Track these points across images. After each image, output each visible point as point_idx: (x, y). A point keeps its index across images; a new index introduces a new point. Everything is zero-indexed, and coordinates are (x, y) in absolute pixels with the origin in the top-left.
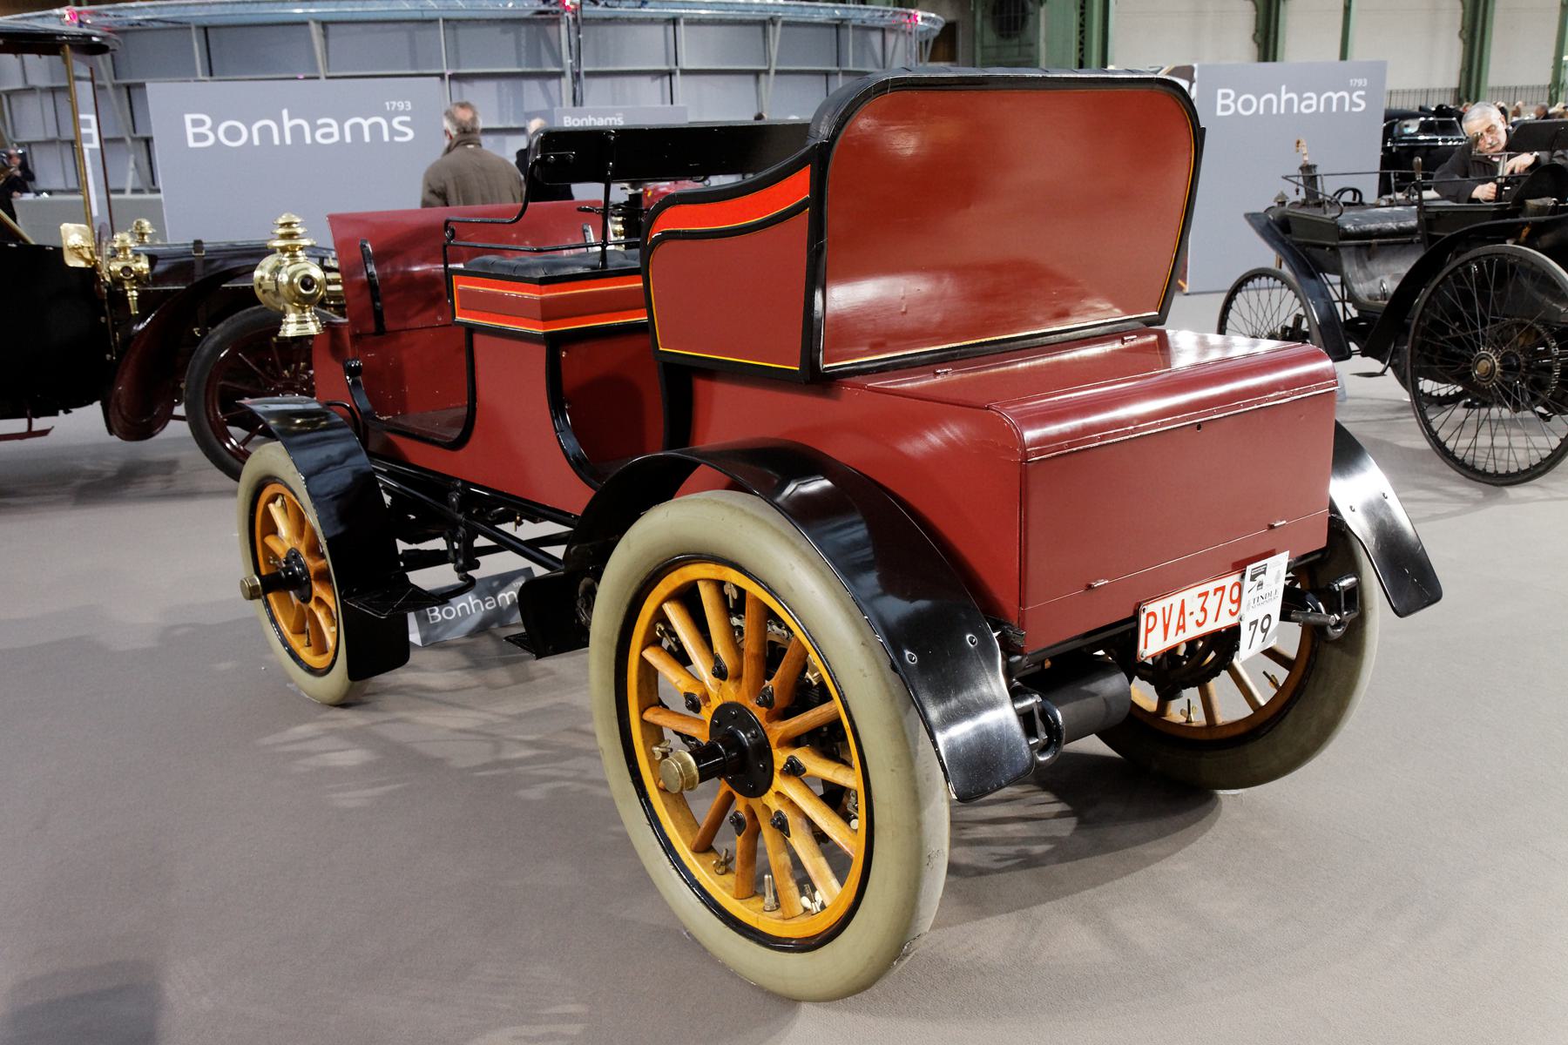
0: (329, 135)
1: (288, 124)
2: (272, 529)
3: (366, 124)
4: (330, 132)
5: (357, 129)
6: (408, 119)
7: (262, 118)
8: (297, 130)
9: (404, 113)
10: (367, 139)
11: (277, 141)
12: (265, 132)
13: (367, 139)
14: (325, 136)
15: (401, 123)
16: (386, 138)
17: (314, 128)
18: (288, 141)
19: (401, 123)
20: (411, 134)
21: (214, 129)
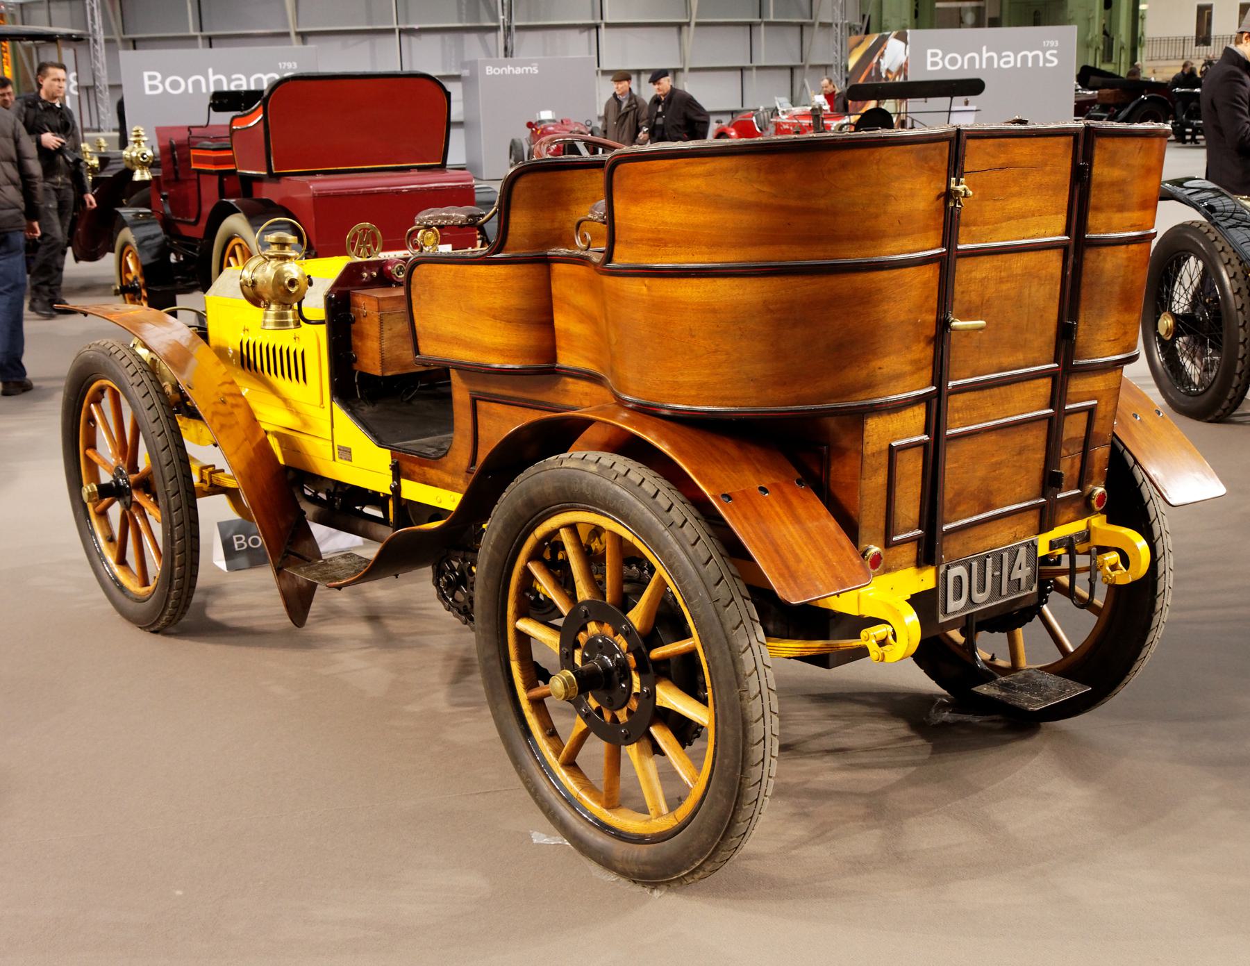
0: (1008, 62)
1: (985, 55)
2: (128, 271)
3: (1030, 55)
5: (1025, 58)
8: (990, 59)
9: (1053, 48)
10: (1030, 65)
11: (977, 66)
12: (972, 60)
13: (1030, 65)
16: (1041, 64)
17: (1000, 58)
18: (984, 66)
20: (1056, 61)
21: (943, 59)
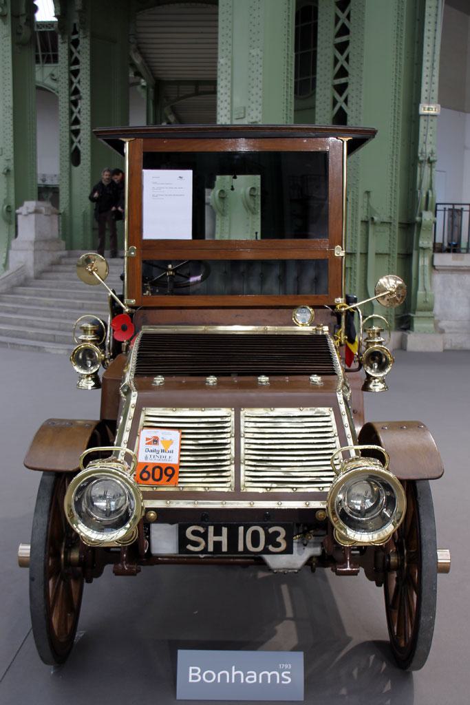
1: (234, 673)
4: (253, 677)
5: (265, 677)
6: (289, 673)
7: (222, 670)
8: (238, 676)
9: (287, 670)
10: (269, 682)
12: (225, 675)
13: (269, 682)
14: (250, 679)
15: (285, 675)
16: (278, 682)
17: (245, 676)
18: (233, 681)
19: (285, 675)
21: (201, 674)
